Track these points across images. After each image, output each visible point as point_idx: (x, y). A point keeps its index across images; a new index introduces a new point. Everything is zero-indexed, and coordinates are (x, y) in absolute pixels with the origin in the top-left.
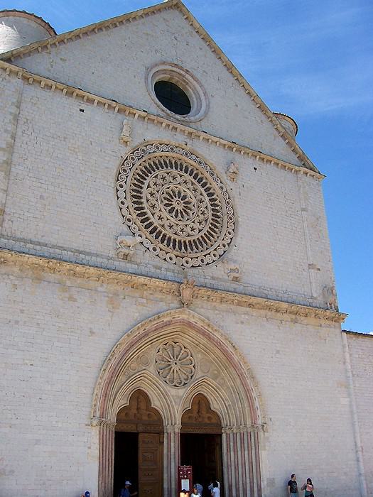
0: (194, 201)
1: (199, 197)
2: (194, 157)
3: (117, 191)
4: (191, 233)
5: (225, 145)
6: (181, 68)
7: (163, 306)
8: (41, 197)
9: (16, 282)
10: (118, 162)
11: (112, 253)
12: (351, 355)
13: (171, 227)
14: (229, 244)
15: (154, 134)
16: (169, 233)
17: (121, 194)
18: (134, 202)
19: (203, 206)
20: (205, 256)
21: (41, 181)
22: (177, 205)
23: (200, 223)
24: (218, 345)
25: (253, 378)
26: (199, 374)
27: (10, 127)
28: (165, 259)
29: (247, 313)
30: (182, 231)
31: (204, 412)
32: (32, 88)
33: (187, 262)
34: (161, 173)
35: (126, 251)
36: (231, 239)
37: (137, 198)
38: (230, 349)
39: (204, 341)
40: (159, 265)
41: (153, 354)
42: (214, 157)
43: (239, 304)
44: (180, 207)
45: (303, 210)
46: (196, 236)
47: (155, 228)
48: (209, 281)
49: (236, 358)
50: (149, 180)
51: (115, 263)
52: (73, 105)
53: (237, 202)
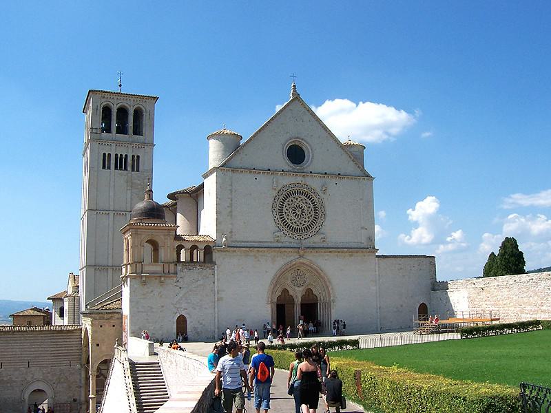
6: (300, 138)
7: (292, 258)
8: (245, 223)
12: (379, 267)
15: (286, 181)
16: (295, 226)
17: (275, 213)
23: (308, 218)
24: (316, 270)
25: (329, 282)
26: (308, 281)
27: (230, 196)
29: (328, 255)
34: (290, 199)
39: (310, 268)
41: (289, 275)
42: (314, 183)
43: (325, 252)
45: (361, 199)
46: (307, 224)
48: (312, 245)
53: (326, 204)
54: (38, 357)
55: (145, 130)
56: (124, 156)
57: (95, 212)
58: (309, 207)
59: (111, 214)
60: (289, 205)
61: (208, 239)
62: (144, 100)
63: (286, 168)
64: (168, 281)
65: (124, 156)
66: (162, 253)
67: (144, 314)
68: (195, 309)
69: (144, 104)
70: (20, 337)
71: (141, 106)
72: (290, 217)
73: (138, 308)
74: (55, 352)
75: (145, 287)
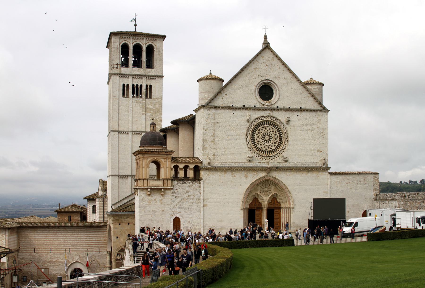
0: (273, 135)
1: (275, 133)
2: (273, 118)
3: (247, 139)
4: (271, 148)
5: (285, 110)
9: (220, 174)
10: (247, 129)
11: (246, 161)
13: (264, 147)
14: (285, 149)
16: (264, 149)
17: (248, 140)
18: (252, 141)
19: (276, 136)
20: (276, 155)
21: (224, 143)
22: (267, 138)
23: (275, 143)
28: (262, 159)
30: (268, 147)
31: (276, 202)
32: (218, 110)
33: (270, 158)
35: (250, 159)
36: (286, 146)
37: (253, 139)
38: (282, 185)
40: (260, 162)
44: (268, 139)
45: (318, 128)
46: (273, 148)
47: (259, 148)
49: (284, 188)
50: (257, 132)
51: (247, 164)
52: (230, 112)
53: (289, 132)
54: (76, 245)
55: (156, 63)
56: (139, 86)
57: (117, 133)
58: (275, 135)
59: (130, 134)
60: (259, 133)
61: (197, 161)
62: (155, 39)
63: (258, 105)
64: (168, 192)
65: (139, 86)
66: (162, 171)
67: (149, 216)
68: (186, 212)
69: (155, 42)
70: (63, 230)
71: (152, 44)
72: (260, 143)
73: (145, 212)
74: (88, 242)
75: (151, 196)
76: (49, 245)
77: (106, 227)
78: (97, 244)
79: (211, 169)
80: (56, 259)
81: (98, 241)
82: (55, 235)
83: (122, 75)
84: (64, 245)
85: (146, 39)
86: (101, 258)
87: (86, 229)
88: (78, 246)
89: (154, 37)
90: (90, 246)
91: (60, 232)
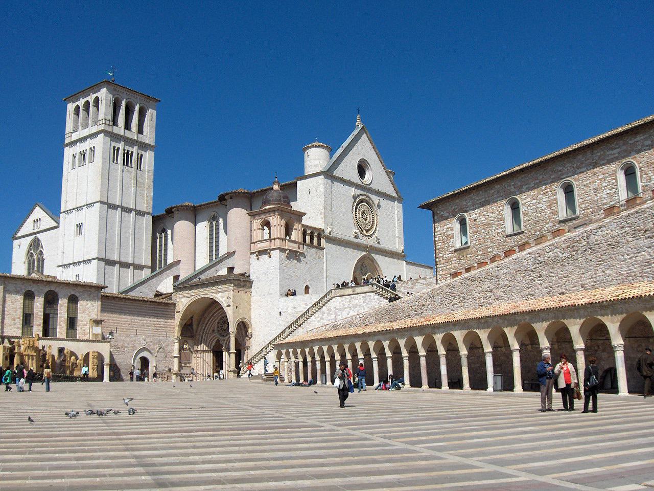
63: (359, 182)
65: (130, 152)
76: (115, 323)
77: (173, 306)
78: (165, 327)
79: (331, 240)
80: (122, 343)
81: (166, 324)
82: (121, 310)
83: (114, 134)
84: (131, 324)
85: (140, 98)
86: (168, 345)
87: (154, 306)
88: (146, 327)
89: (147, 99)
90: (158, 328)
91: (127, 306)
